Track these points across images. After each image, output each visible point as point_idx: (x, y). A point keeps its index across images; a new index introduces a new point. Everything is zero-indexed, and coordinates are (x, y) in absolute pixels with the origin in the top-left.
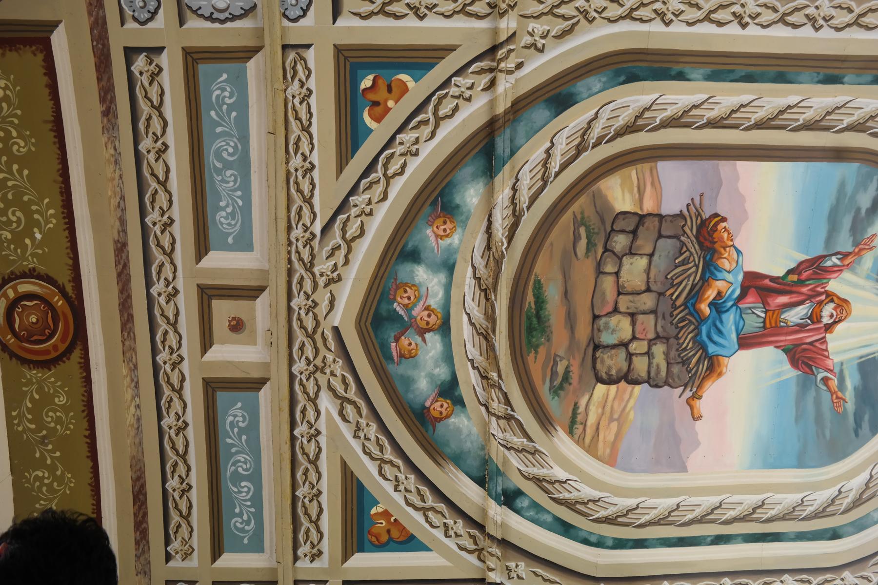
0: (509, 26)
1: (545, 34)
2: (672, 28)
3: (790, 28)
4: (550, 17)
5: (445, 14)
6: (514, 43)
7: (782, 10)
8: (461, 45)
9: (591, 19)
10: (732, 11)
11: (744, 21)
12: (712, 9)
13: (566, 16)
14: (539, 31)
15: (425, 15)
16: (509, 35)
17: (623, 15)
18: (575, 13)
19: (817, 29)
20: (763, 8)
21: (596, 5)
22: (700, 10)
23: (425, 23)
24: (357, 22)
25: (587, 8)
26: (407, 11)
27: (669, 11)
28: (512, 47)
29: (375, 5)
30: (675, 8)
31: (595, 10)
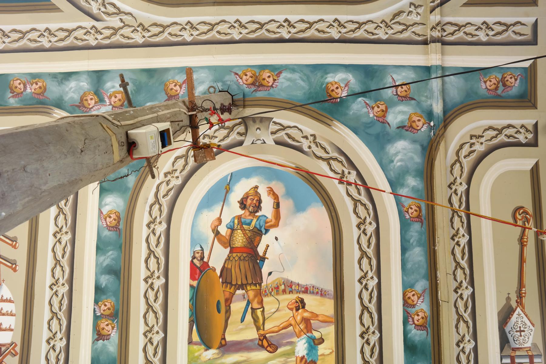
0: (434, 16)
1: (410, 14)
2: (333, 17)
3: (256, 20)
4: (408, 24)
5: (470, 25)
6: (431, 7)
7: (263, 31)
8: (460, 7)
9: (383, 22)
10: (296, 29)
11: (287, 23)
12: (309, 30)
13: (398, 24)
14: (414, 16)
15: (482, 24)
16: (434, 11)
17: (364, 25)
18: (393, 26)
19: (237, 21)
20: (276, 32)
21: (381, 31)
22: (317, 28)
23: (482, 20)
24: (523, 20)
25: (386, 29)
26: (493, 27)
27: (336, 28)
28: (432, 4)
29: (512, 30)
30: (333, 29)
31: (381, 28)
